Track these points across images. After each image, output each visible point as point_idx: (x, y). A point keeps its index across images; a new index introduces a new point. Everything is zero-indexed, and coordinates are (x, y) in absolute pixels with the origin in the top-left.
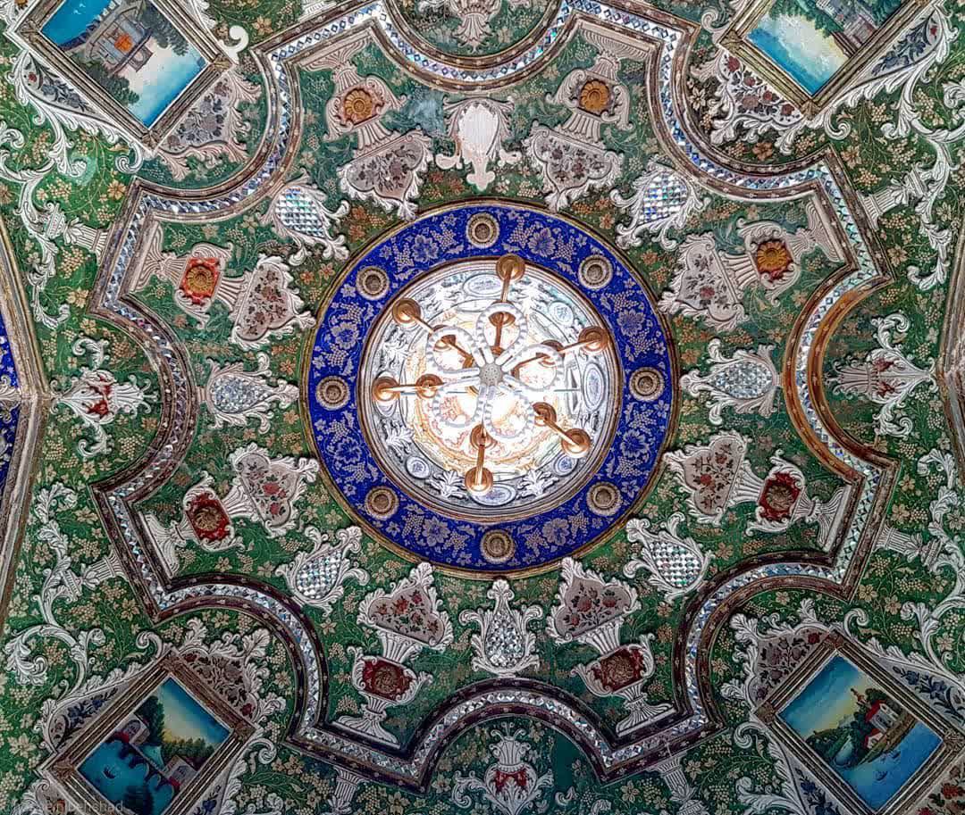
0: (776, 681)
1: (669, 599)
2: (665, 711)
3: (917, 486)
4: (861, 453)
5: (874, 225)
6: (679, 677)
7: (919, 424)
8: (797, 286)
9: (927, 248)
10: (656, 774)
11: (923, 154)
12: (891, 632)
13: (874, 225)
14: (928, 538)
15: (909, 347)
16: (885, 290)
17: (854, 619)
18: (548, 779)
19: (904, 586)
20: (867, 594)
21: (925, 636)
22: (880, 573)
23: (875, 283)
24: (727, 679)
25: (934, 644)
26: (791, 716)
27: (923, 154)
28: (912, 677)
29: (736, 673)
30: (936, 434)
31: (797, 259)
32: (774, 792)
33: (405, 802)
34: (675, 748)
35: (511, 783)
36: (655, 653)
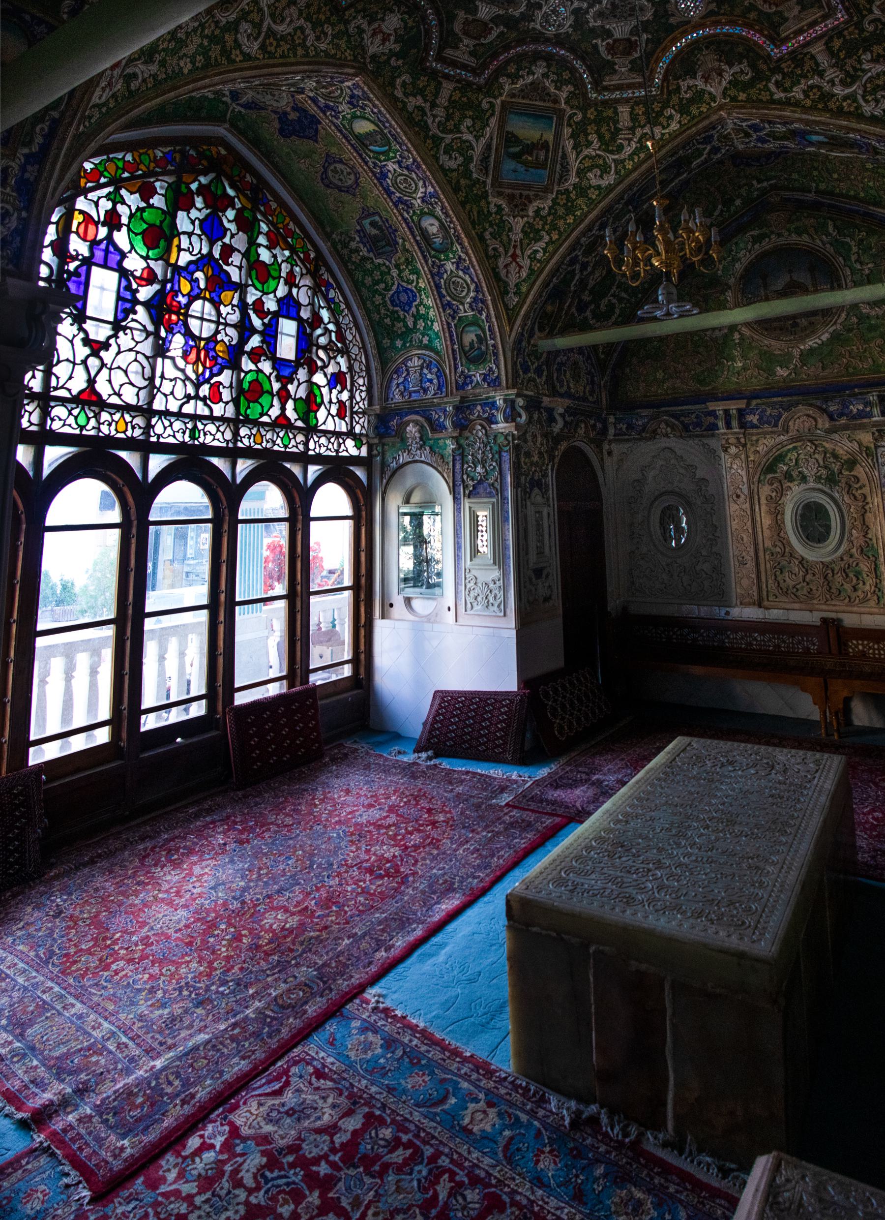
0: (523, 98)
1: (532, 25)
2: (472, 62)
3: (657, 113)
4: (665, 79)
5: (805, 51)
6: (495, 56)
7: (691, 101)
8: (760, 12)
9: (794, 84)
10: (440, 83)
11: (850, 79)
12: (580, 133)
13: (805, 51)
14: (632, 129)
15: (734, 83)
16: (765, 62)
17: (575, 114)
18: (397, 48)
19: (604, 129)
20: (591, 114)
21: (586, 152)
22: (605, 114)
23: (769, 56)
24: (509, 76)
25: (584, 159)
26: (512, 116)
27: (850, 79)
28: (564, 156)
29: (515, 78)
30: (688, 113)
31: (779, 9)
32: (475, 136)
33: (328, 14)
34: (458, 81)
35: (380, 37)
36: (498, 37)
